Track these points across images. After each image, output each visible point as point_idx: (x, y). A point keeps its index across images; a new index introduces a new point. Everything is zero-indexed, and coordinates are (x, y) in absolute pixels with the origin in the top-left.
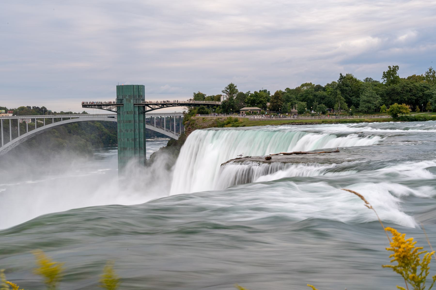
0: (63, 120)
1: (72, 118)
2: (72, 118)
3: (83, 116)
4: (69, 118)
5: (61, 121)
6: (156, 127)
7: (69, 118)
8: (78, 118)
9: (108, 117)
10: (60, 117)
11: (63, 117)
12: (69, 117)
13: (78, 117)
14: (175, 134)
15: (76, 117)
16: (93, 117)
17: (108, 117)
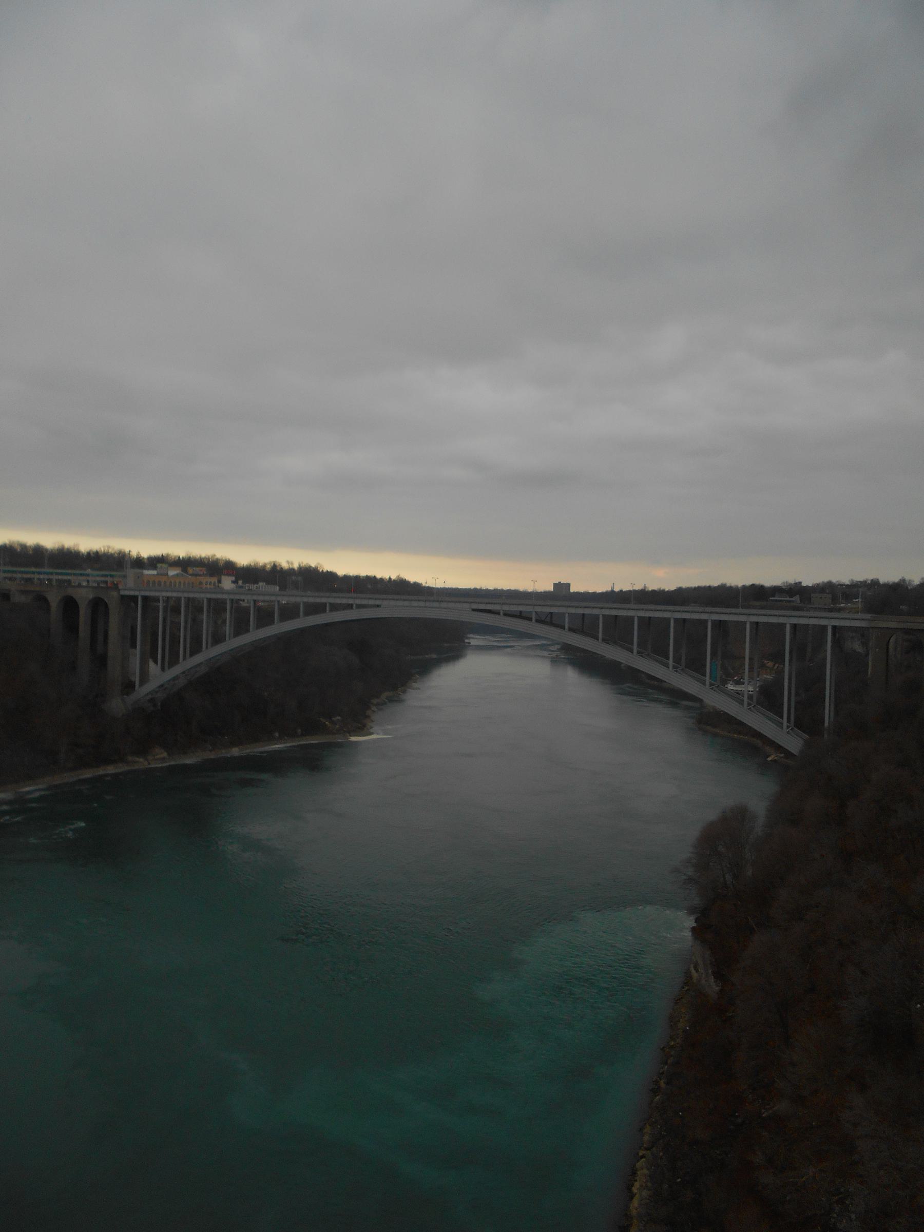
0: (331, 610)
1: (360, 606)
2: (360, 606)
3: (393, 603)
4: (350, 606)
5: (324, 611)
6: (603, 640)
7: (350, 606)
8: (378, 606)
9: (474, 610)
10: (324, 600)
11: (332, 600)
12: (351, 601)
13: (378, 602)
14: (707, 683)
15: (371, 602)
16: (425, 607)
17: (474, 610)
